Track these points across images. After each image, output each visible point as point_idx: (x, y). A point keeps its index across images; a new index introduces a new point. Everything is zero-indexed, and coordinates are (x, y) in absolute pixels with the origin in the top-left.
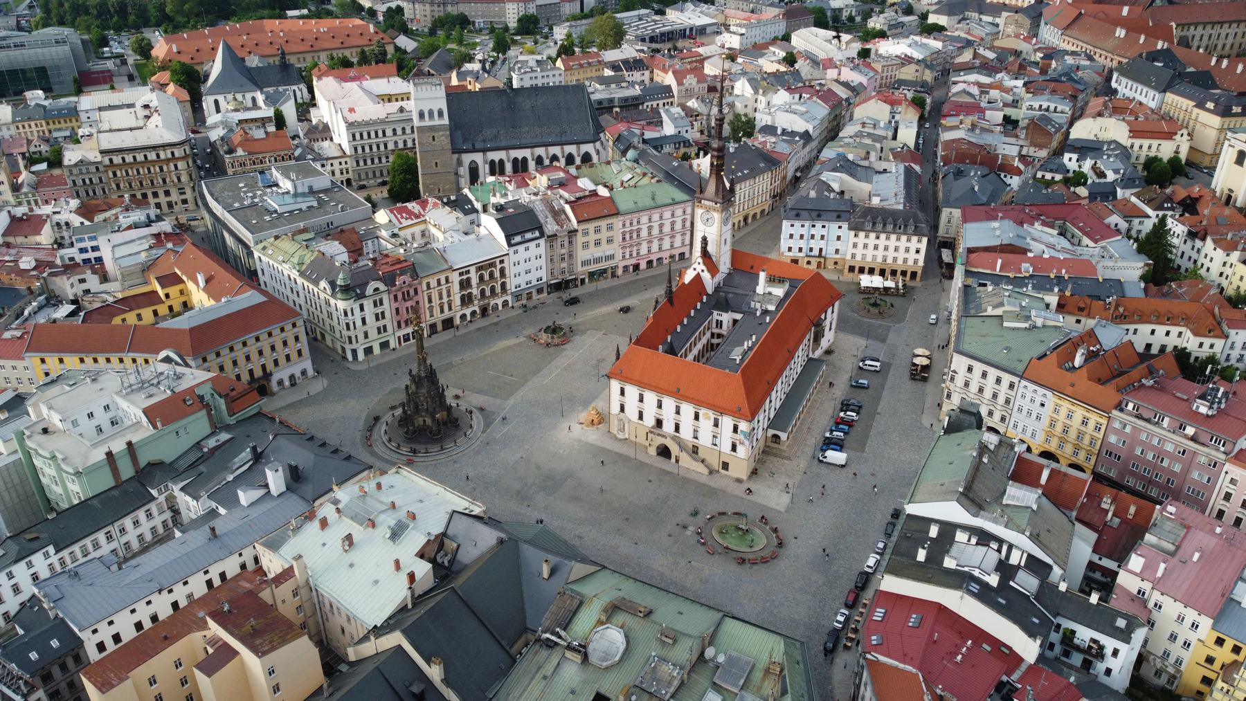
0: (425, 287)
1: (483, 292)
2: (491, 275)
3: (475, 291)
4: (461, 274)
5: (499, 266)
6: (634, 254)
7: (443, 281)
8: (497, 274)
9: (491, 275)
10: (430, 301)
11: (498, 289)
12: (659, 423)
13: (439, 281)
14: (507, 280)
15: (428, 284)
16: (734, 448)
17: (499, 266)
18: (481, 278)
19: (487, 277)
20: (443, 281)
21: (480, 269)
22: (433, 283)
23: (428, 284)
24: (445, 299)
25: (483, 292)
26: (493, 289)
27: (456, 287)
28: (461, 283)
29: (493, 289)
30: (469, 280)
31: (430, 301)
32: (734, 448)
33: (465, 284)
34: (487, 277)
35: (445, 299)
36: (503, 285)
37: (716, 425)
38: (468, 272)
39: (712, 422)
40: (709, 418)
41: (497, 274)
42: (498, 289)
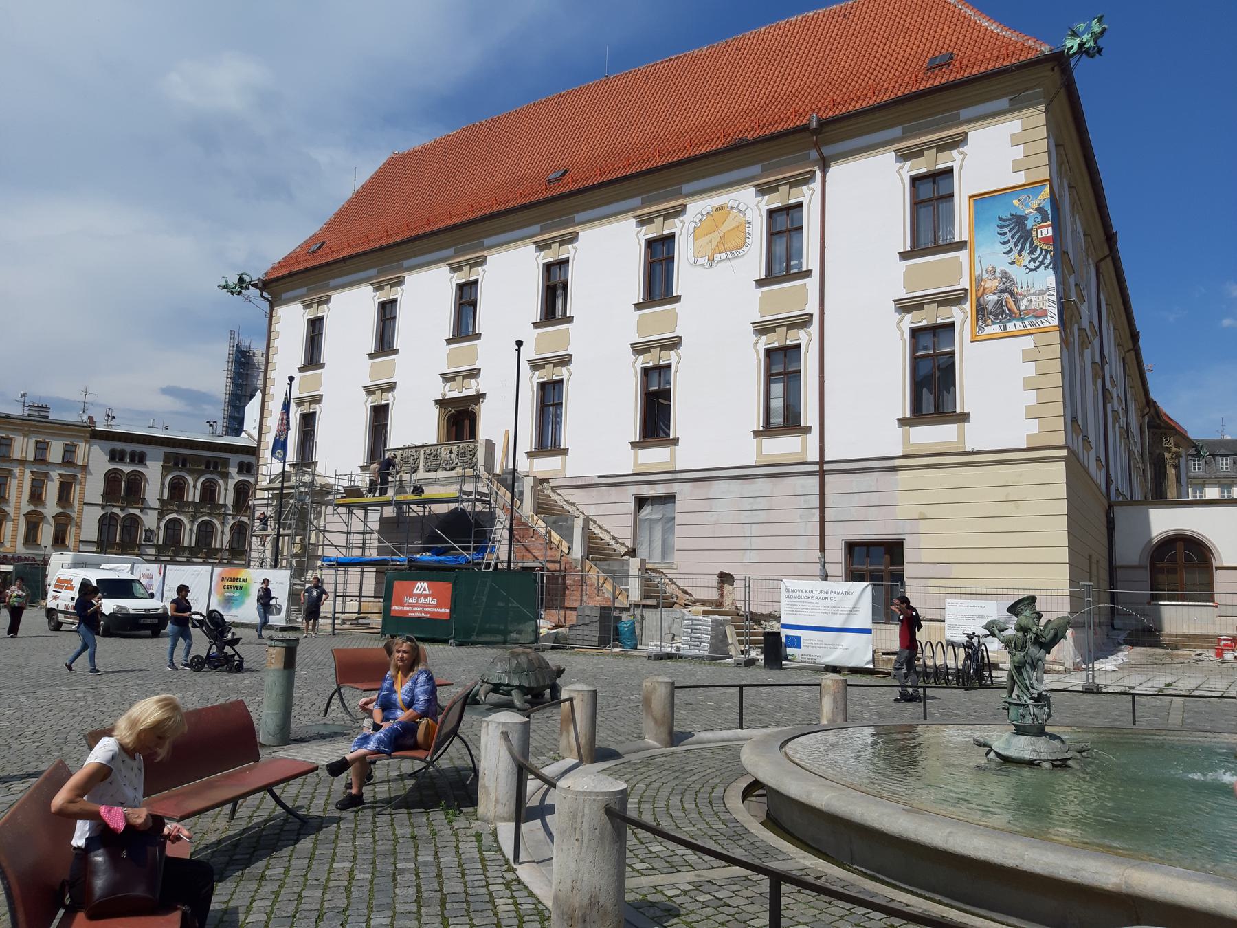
1: (174, 528)
2: (209, 492)
3: (150, 520)
5: (235, 477)
8: (226, 495)
9: (209, 492)
11: (222, 538)
12: (460, 418)
13: (42, 447)
16: (932, 385)
18: (177, 489)
19: (193, 493)
24: (51, 508)
25: (174, 528)
26: (205, 532)
27: (93, 488)
28: (112, 479)
29: (205, 532)
30: (136, 484)
32: (932, 385)
33: (124, 489)
34: (193, 493)
35: (51, 508)
36: (240, 532)
37: (782, 264)
38: (140, 459)
39: (754, 260)
40: (731, 247)
41: (226, 495)
42: (222, 538)
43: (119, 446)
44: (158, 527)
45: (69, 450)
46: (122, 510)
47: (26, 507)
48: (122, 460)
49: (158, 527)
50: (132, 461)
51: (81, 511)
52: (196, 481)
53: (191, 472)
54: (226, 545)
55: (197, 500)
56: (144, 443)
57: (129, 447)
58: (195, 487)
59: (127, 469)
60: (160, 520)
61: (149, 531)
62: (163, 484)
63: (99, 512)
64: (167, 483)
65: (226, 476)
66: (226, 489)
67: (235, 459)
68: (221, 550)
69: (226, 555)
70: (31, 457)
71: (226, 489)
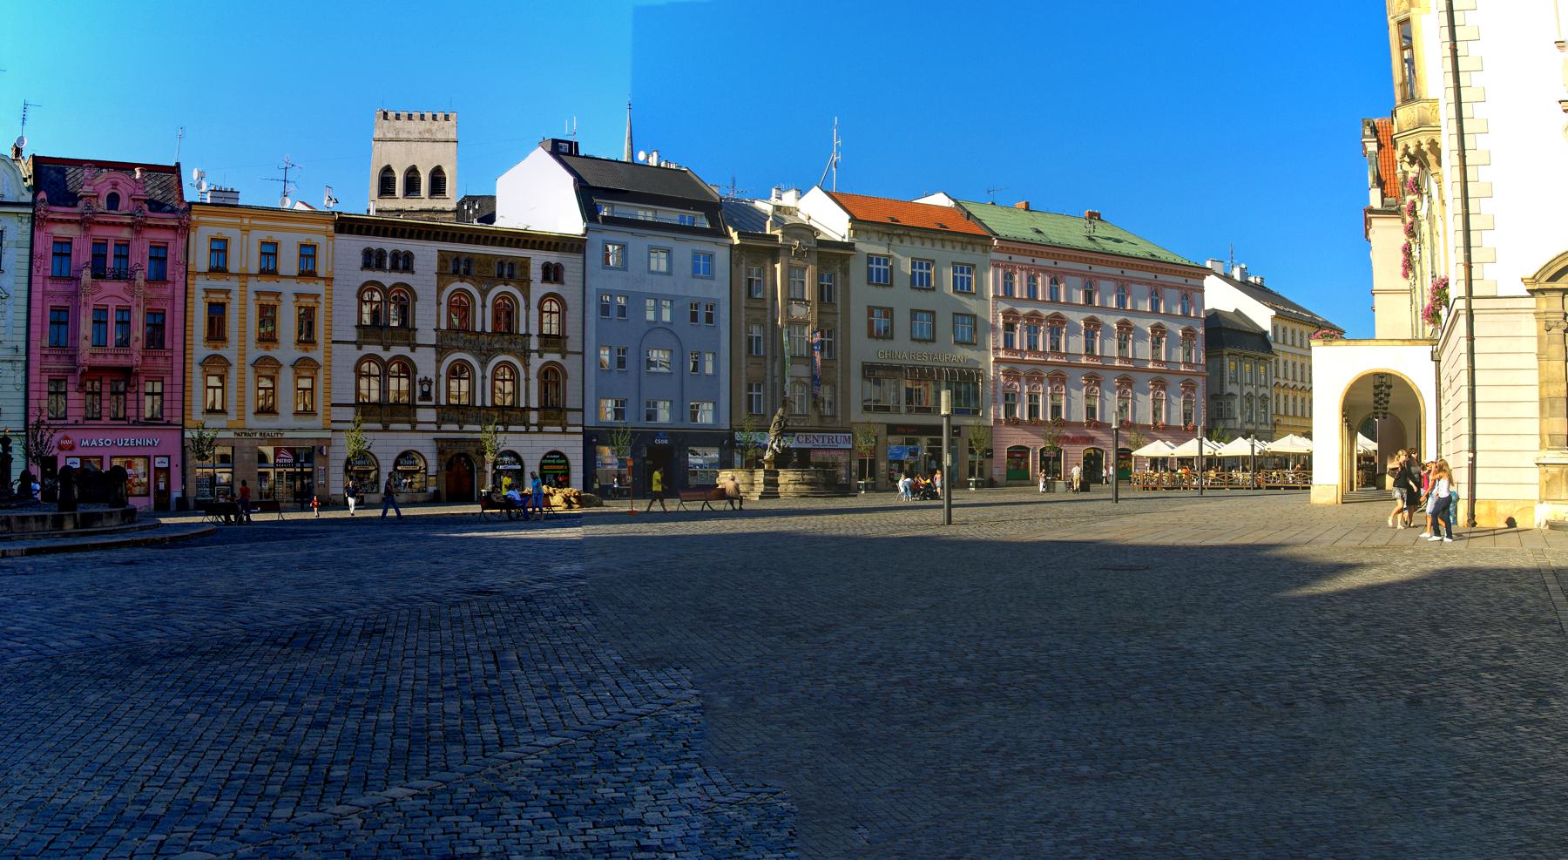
0: (201, 258)
4: (372, 260)
6: (1045, 414)
7: (289, 262)
10: (216, 331)
13: (270, 251)
14: (572, 365)
15: (220, 248)
17: (539, 288)
19: (483, 319)
20: (289, 262)
21: (452, 267)
22: (244, 256)
23: (220, 248)
30: (404, 300)
31: (216, 331)
34: (483, 319)
38: (404, 262)
43: (376, 243)
44: (438, 376)
45: (308, 252)
46: (387, 349)
47: (255, 352)
48: (380, 266)
49: (438, 376)
50: (394, 268)
51: (328, 353)
52: (484, 294)
53: (476, 281)
54: (534, 403)
55: (489, 329)
56: (411, 237)
57: (390, 245)
58: (484, 306)
59: (388, 279)
60: (439, 362)
61: (427, 381)
62: (439, 304)
63: (354, 354)
64: (444, 300)
65: (524, 284)
66: (528, 307)
67: (537, 259)
68: (528, 408)
69: (534, 417)
70: (255, 269)
71: (528, 307)
